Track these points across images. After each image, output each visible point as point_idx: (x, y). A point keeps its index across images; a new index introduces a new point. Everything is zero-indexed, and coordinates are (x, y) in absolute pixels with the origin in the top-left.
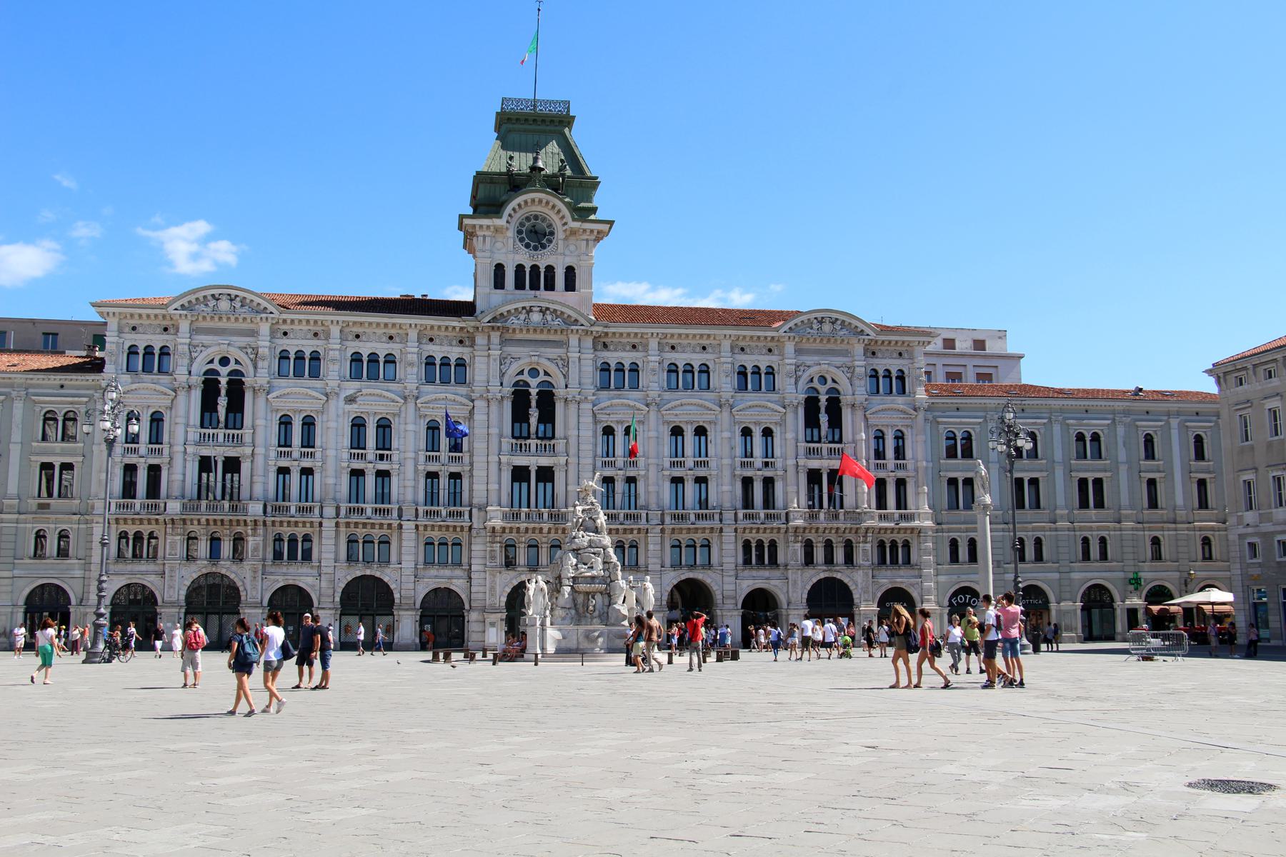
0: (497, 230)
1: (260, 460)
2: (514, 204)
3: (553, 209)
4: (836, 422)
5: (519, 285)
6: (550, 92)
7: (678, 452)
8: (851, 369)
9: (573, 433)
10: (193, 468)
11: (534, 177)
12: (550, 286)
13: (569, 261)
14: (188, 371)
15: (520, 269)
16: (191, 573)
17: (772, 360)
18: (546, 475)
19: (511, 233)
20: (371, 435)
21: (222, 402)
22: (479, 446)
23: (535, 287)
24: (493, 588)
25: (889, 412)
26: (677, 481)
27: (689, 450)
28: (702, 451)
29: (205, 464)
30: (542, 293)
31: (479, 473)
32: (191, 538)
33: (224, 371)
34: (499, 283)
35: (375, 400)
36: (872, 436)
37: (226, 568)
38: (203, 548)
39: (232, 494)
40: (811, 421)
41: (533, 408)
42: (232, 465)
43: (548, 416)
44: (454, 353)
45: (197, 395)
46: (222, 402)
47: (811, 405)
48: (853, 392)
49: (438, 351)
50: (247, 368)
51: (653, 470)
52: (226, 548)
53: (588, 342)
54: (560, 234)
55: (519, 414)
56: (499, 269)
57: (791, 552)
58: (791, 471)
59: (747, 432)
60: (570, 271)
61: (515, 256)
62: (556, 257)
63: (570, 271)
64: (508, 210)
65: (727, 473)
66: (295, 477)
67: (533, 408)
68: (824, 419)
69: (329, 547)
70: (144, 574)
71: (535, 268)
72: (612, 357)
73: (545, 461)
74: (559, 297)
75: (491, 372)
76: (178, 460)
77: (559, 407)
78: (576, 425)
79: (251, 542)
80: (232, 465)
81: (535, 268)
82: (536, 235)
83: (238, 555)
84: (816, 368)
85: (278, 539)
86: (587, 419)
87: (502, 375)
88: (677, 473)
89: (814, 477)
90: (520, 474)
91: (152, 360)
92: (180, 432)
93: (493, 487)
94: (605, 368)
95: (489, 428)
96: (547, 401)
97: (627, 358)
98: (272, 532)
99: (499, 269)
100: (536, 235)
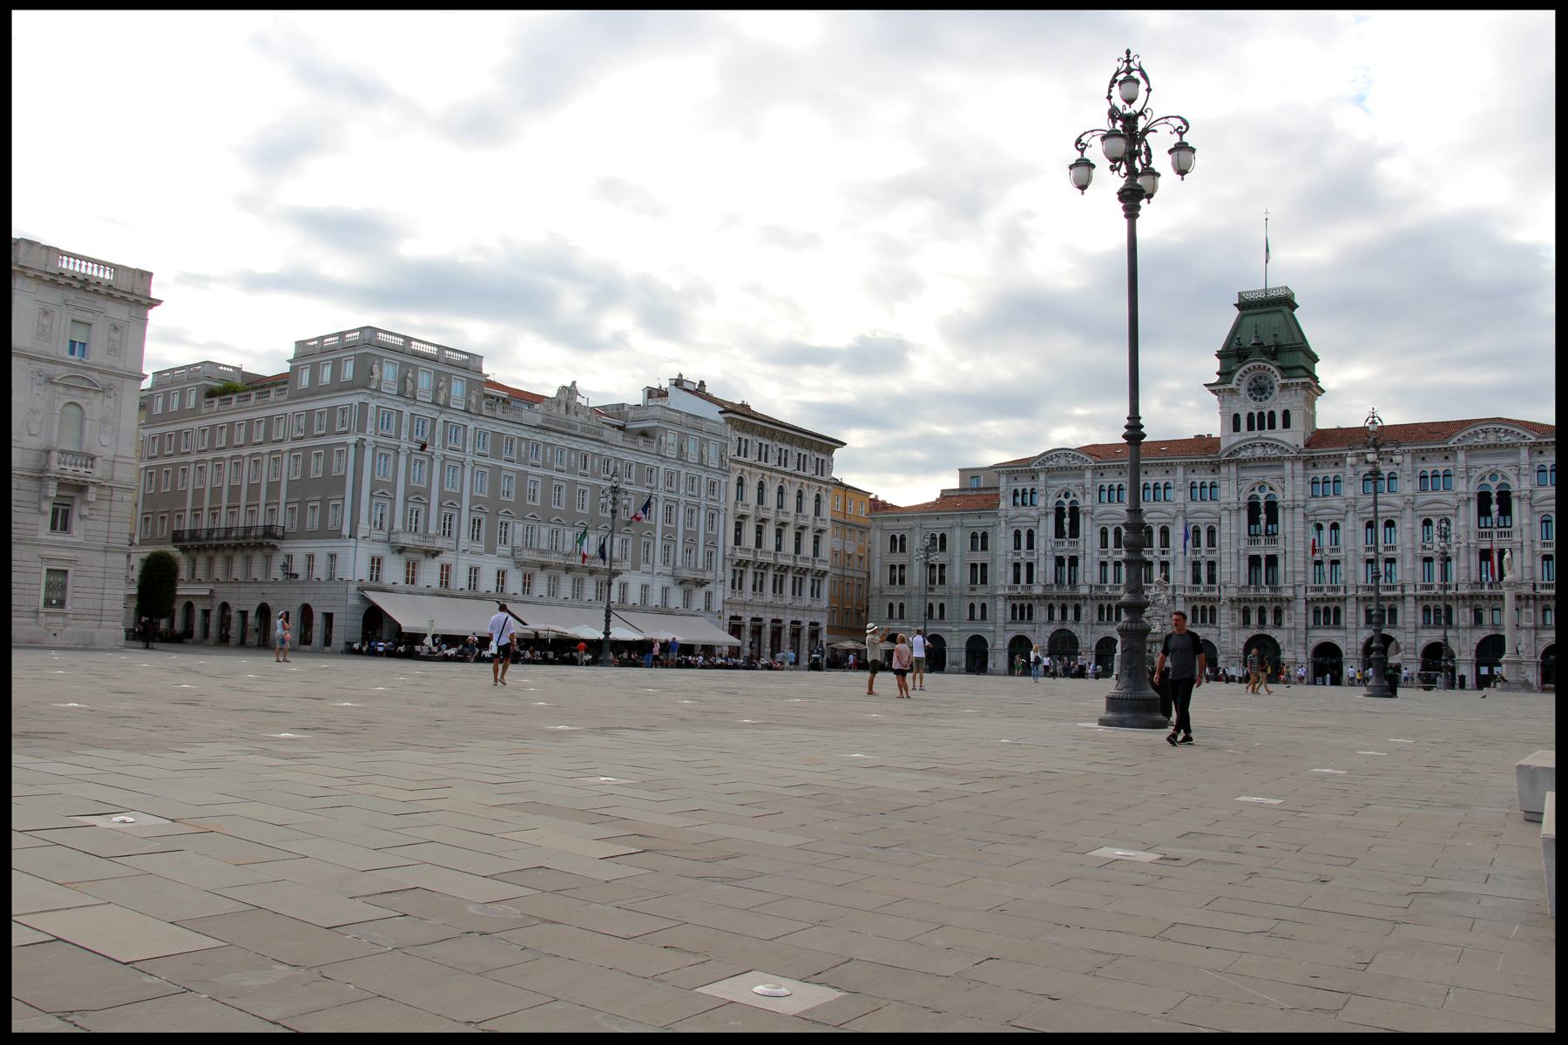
0: (1232, 390)
1: (1088, 558)
2: (1241, 371)
4: (1506, 510)
5: (1250, 428)
6: (1277, 282)
8: (1517, 466)
9: (1288, 529)
10: (1051, 565)
11: (1266, 345)
12: (1272, 426)
13: (1285, 407)
15: (1250, 416)
16: (1052, 629)
17: (1448, 465)
18: (1272, 561)
19: (1243, 390)
21: (1067, 520)
22: (1225, 540)
23: (1261, 428)
24: (1233, 642)
27: (1381, 540)
29: (1059, 561)
30: (1267, 433)
31: (1225, 559)
32: (1051, 608)
33: (1067, 502)
34: (1236, 428)
36: (1538, 519)
38: (1057, 614)
39: (1073, 582)
40: (1484, 510)
41: (1263, 513)
42: (1074, 561)
43: (1273, 519)
45: (1052, 518)
46: (1067, 520)
47: (1484, 500)
49: (1198, 478)
50: (1080, 500)
51: (1350, 555)
52: (1070, 614)
53: (1299, 466)
54: (1277, 389)
55: (1253, 519)
56: (1236, 418)
57: (1463, 616)
58: (1462, 551)
59: (1427, 523)
60: (1286, 414)
62: (1276, 404)
63: (1286, 414)
64: (1237, 376)
65: (1409, 557)
66: (1110, 569)
67: (1263, 513)
68: (1494, 507)
70: (1024, 629)
71: (1261, 415)
72: (1320, 473)
73: (1271, 552)
74: (1279, 434)
75: (1231, 490)
76: (1042, 558)
77: (1280, 512)
78: (1291, 526)
79: (1083, 611)
81: (1261, 415)
82: (1260, 390)
83: (1077, 617)
84: (1485, 469)
85: (1101, 609)
86: (1300, 518)
87: (1239, 492)
88: (1427, 554)
90: (1254, 561)
91: (1023, 498)
92: (1042, 541)
93: (1234, 569)
94: (1314, 482)
95: (1233, 529)
96: (1272, 508)
97: (1331, 473)
98: (1096, 605)
99: (1236, 418)
100: (1260, 390)
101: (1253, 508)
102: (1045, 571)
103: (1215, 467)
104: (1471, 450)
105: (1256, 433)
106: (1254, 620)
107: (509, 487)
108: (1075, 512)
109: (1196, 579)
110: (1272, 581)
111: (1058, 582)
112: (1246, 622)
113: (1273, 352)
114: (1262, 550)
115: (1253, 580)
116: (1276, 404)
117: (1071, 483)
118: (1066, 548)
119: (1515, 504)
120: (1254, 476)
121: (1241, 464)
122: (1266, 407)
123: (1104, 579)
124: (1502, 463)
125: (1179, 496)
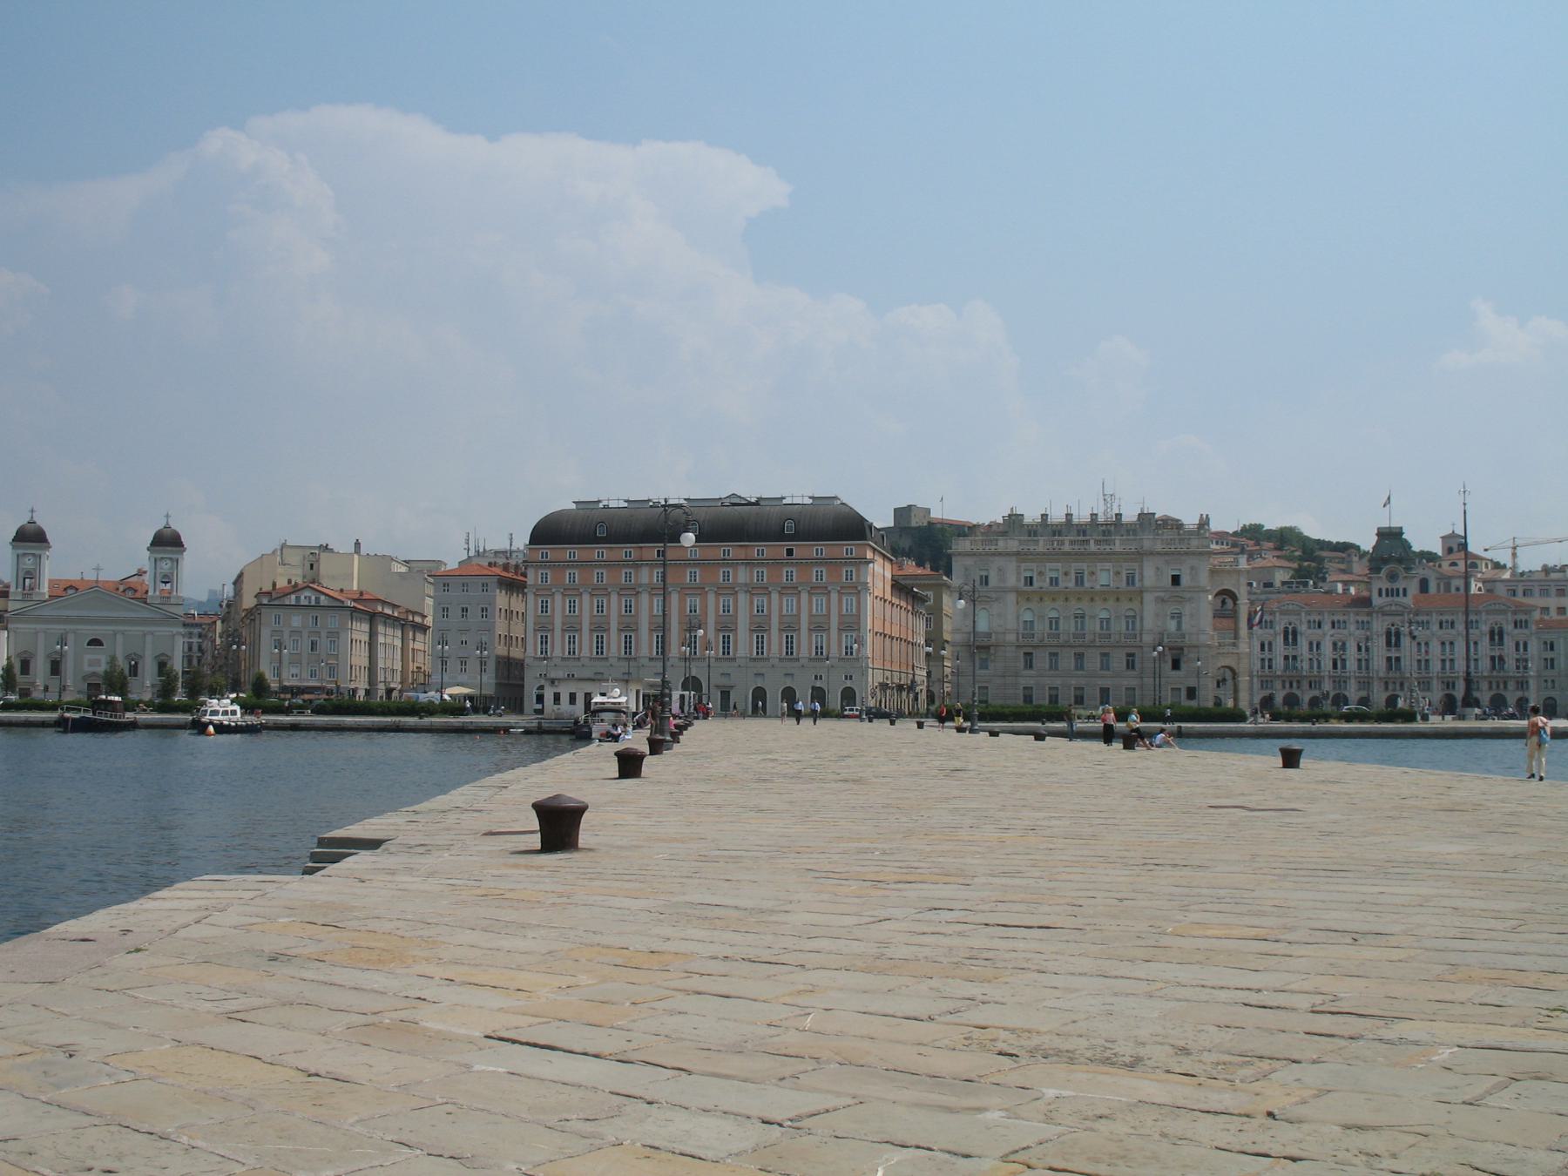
3: (1400, 569)
4: (1501, 638)
7: (1443, 650)
14: (1279, 628)
18: (1398, 659)
20: (1340, 647)
25: (1520, 634)
26: (1443, 661)
28: (1452, 650)
29: (1286, 658)
30: (1396, 599)
35: (1339, 634)
37: (1295, 691)
40: (1492, 639)
42: (1295, 658)
44: (1365, 619)
47: (1492, 633)
48: (1508, 628)
49: (1360, 619)
61: (1385, 585)
62: (1400, 585)
69: (1327, 686)
74: (1401, 599)
80: (1295, 658)
82: (1392, 577)
89: (1493, 658)
90: (1389, 659)
97: (1425, 618)
100: (1392, 577)
101: (1388, 634)
102: (1279, 663)
103: (1370, 614)
104: (1488, 612)
105: (1390, 599)
106: (1391, 687)
107: (1093, 626)
108: (1295, 633)
109: (1360, 668)
110: (1398, 668)
111: (1286, 667)
112: (1387, 689)
113: (1400, 561)
114: (1393, 654)
115: (1390, 668)
116: (1400, 585)
117: (1293, 618)
118: (1290, 652)
119: (1505, 637)
120: (1389, 619)
121: (1384, 614)
122: (1395, 586)
123: (1311, 667)
124: (1499, 618)
125: (1352, 628)
